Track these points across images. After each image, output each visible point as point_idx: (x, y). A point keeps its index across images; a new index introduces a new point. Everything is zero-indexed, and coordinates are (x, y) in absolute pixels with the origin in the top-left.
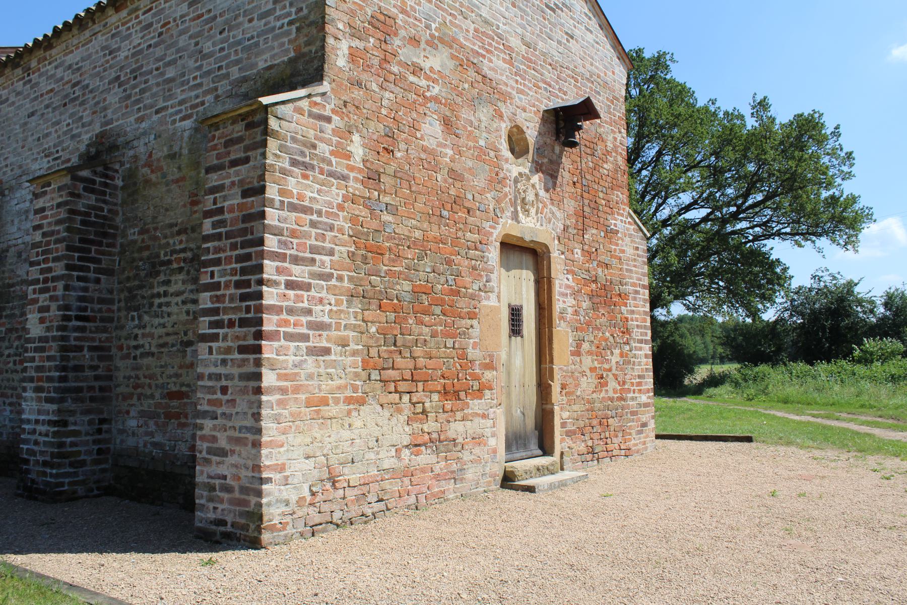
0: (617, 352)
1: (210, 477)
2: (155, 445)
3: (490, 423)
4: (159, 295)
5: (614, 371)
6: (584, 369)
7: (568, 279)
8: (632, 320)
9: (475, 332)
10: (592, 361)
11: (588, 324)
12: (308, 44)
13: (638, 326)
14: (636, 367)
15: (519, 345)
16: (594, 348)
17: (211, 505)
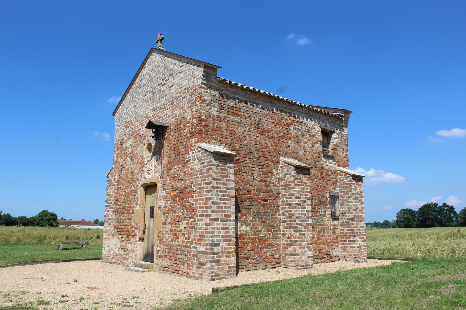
0: (185, 222)
3: (136, 246)
5: (183, 232)
6: (167, 230)
7: (163, 193)
8: (196, 204)
9: (133, 218)
10: (172, 227)
11: (170, 210)
13: (200, 208)
14: (197, 231)
15: (153, 221)
16: (172, 221)
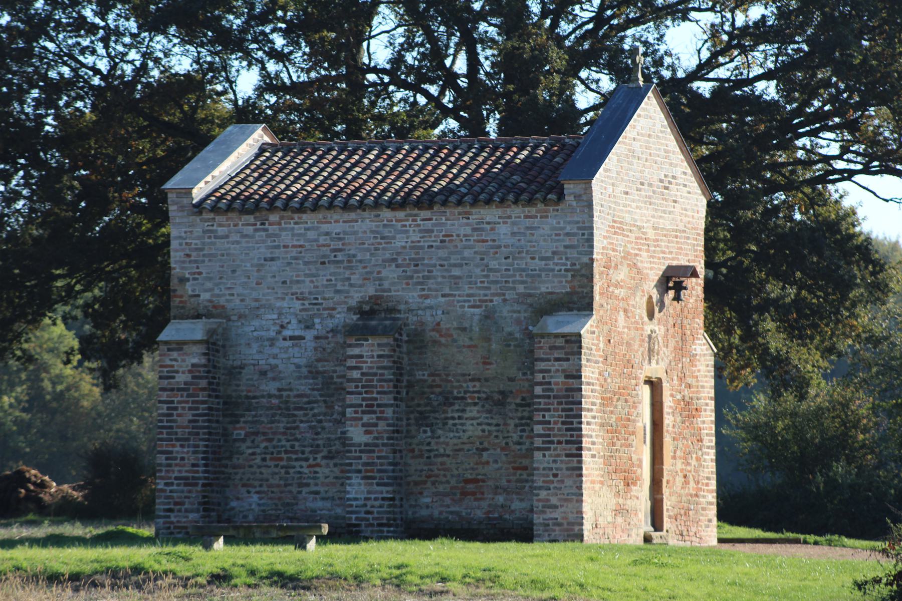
1: (544, 519)
2: (451, 513)
4: (453, 418)
12: (580, 287)
17: (546, 534)
